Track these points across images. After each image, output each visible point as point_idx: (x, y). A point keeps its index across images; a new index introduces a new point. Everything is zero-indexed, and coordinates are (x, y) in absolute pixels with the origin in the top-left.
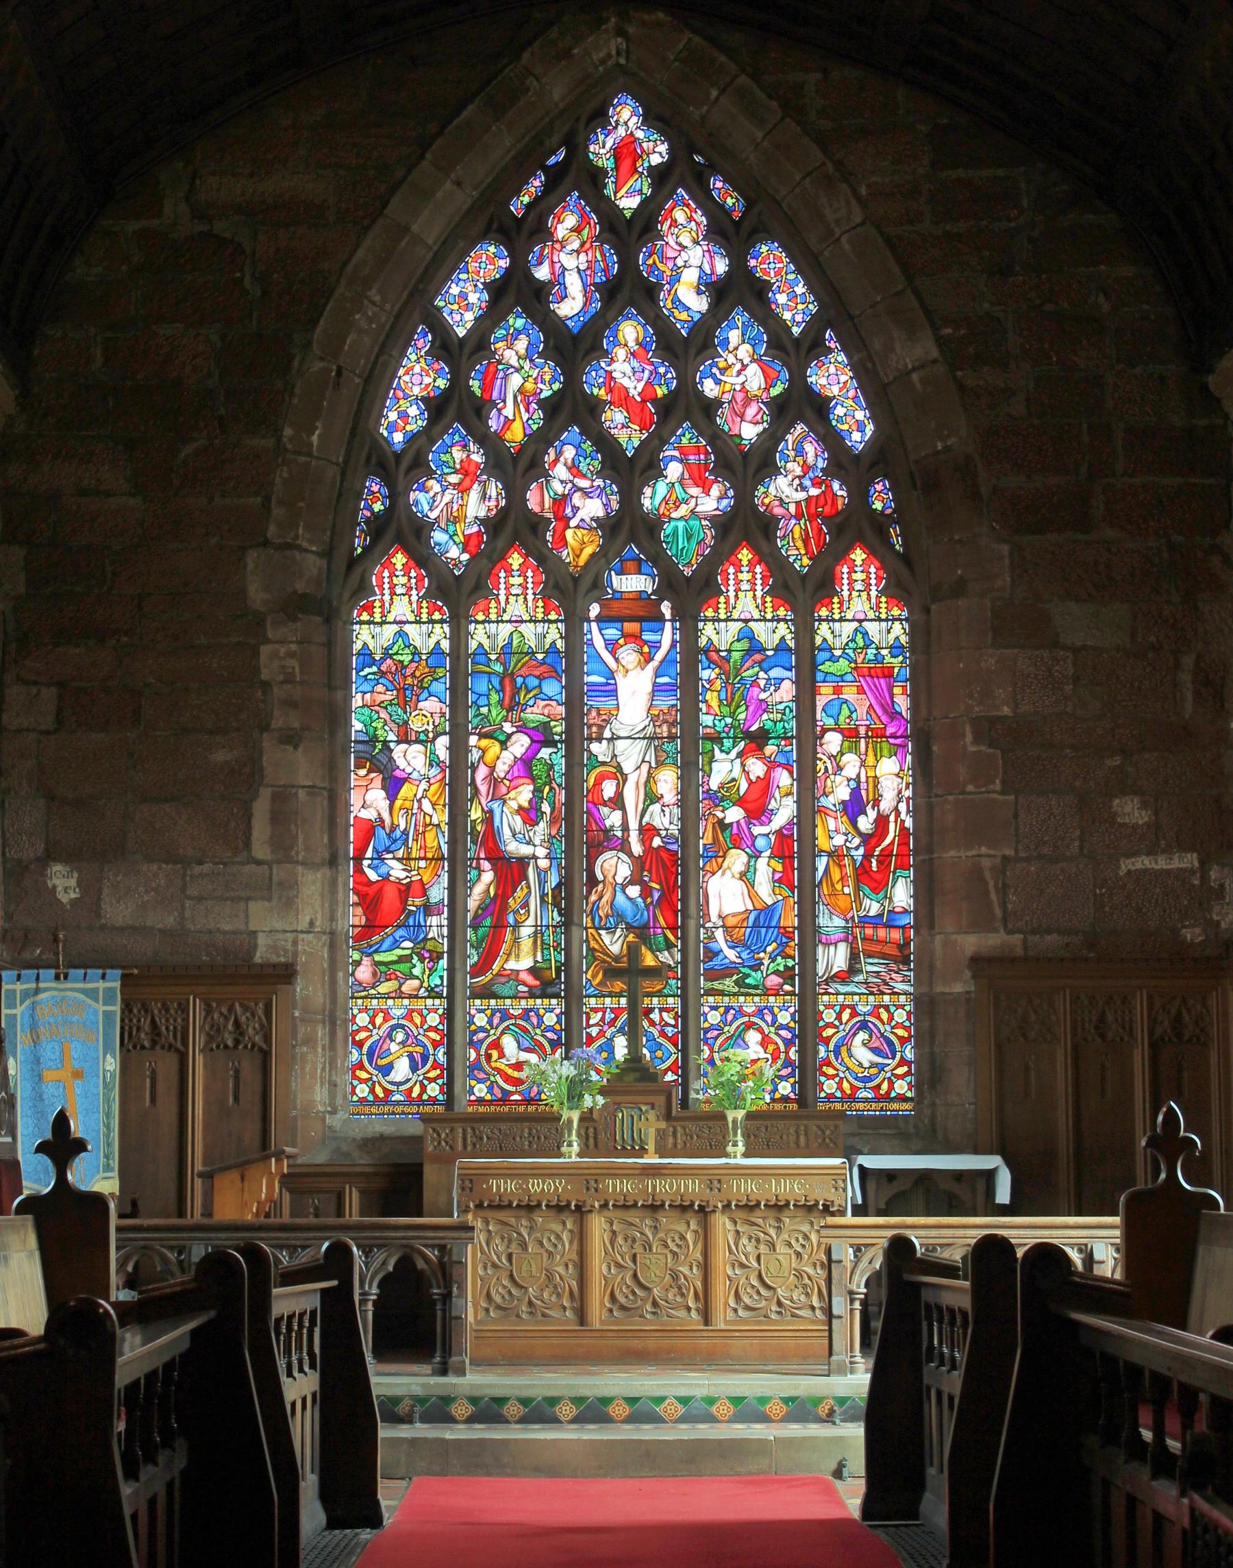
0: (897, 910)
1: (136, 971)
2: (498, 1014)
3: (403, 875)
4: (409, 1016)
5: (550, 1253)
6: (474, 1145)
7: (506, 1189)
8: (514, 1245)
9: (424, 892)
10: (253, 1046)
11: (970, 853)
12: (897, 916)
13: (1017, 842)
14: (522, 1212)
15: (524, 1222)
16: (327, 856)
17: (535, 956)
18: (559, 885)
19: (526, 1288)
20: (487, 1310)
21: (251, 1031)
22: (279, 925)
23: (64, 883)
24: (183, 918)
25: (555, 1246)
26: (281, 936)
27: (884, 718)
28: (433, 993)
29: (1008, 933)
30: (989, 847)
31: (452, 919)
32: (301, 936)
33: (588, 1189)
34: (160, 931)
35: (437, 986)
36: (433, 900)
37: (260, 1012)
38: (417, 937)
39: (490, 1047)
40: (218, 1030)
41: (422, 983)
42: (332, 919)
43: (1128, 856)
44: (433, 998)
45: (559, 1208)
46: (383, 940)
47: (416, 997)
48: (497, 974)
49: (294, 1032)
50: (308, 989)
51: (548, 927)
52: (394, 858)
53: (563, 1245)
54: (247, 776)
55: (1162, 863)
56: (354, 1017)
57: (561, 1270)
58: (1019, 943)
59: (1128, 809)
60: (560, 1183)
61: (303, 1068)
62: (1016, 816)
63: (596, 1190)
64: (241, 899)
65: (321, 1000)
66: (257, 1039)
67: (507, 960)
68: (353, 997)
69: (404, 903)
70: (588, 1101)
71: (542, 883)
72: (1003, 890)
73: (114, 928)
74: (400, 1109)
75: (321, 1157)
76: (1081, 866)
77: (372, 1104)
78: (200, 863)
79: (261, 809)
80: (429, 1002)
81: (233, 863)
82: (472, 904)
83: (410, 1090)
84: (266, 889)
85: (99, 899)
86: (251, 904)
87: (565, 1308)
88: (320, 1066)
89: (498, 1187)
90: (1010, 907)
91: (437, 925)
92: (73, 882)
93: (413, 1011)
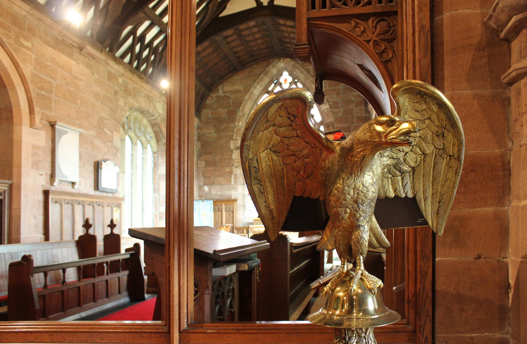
50: (239, 202)
54: (231, 172)
79: (233, 177)
84: (233, 188)
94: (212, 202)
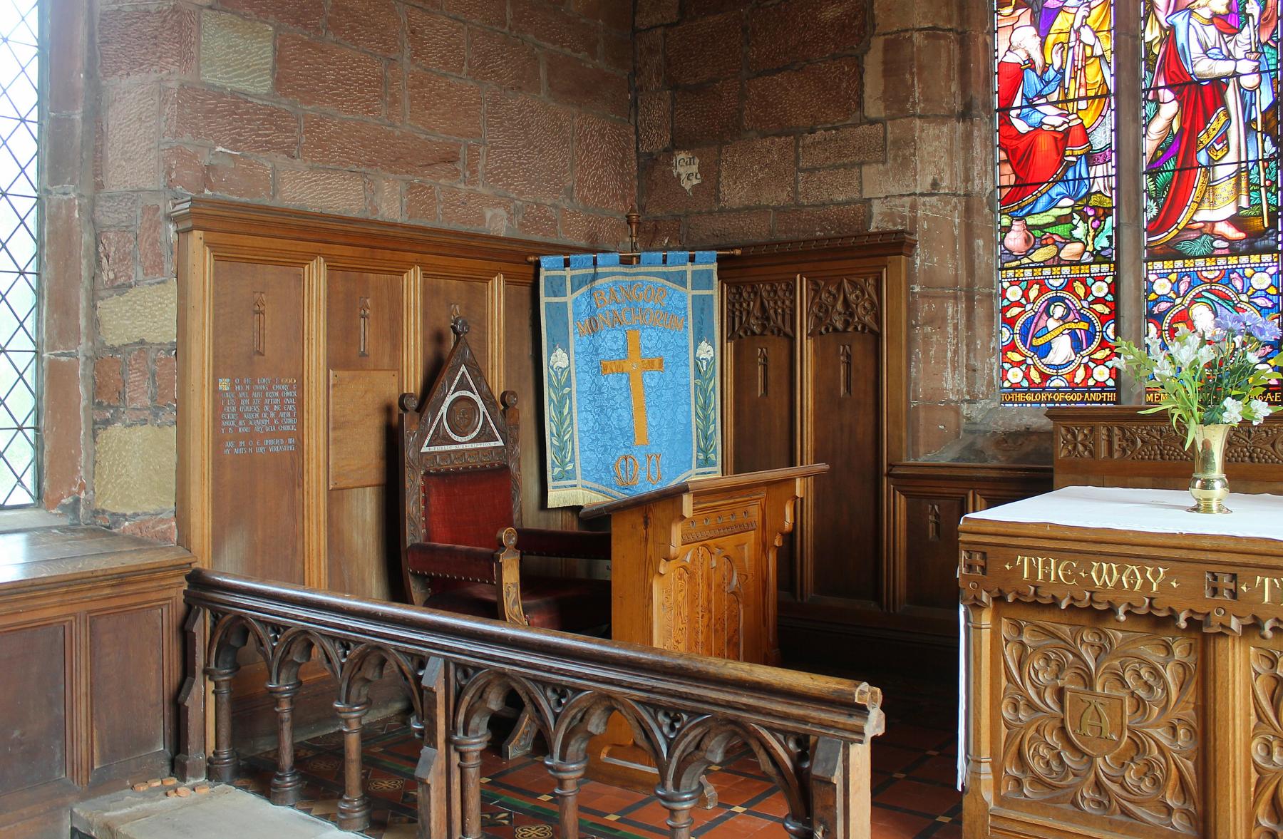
1: (738, 252)
2: (1186, 279)
3: (1057, 121)
4: (1069, 287)
5: (1139, 703)
6: (1124, 450)
7: (1047, 576)
8: (1068, 675)
9: (1086, 136)
10: (864, 328)
14: (1084, 620)
15: (1088, 637)
16: (958, 107)
17: (1237, 200)
18: (1273, 106)
19: (1091, 760)
20: (1018, 782)
21: (860, 311)
22: (895, 191)
23: (687, 170)
24: (796, 192)
25: (1150, 688)
26: (897, 201)
28: (1098, 257)
31: (1117, 167)
32: (923, 199)
33: (1215, 591)
34: (774, 208)
35: (1103, 249)
36: (1097, 146)
37: (870, 289)
38: (1078, 192)
39: (1176, 319)
40: (827, 310)
41: (1085, 246)
42: (967, 179)
44: (1100, 263)
45: (1157, 622)
46: (1037, 200)
47: (1078, 263)
48: (1184, 229)
49: (912, 310)
50: (932, 259)
51: (1256, 162)
52: (1048, 103)
53: (1166, 689)
56: (1004, 291)
57: (1161, 735)
60: (1155, 574)
61: (926, 352)
63: (1234, 594)
64: (853, 165)
65: (951, 272)
66: (867, 319)
67: (1197, 210)
68: (1002, 269)
69: (1062, 154)
70: (1233, 411)
71: (1246, 107)
73: (731, 210)
74: (1060, 397)
75: (946, 456)
77: (1028, 390)
78: (812, 131)
80: (1095, 268)
81: (845, 126)
82: (1149, 145)
83: (1074, 373)
85: (718, 182)
86: (865, 169)
87: (1169, 811)
88: (950, 349)
89: (1033, 571)
91: (1101, 176)
92: (694, 169)
93: (1075, 280)
94: (708, 263)
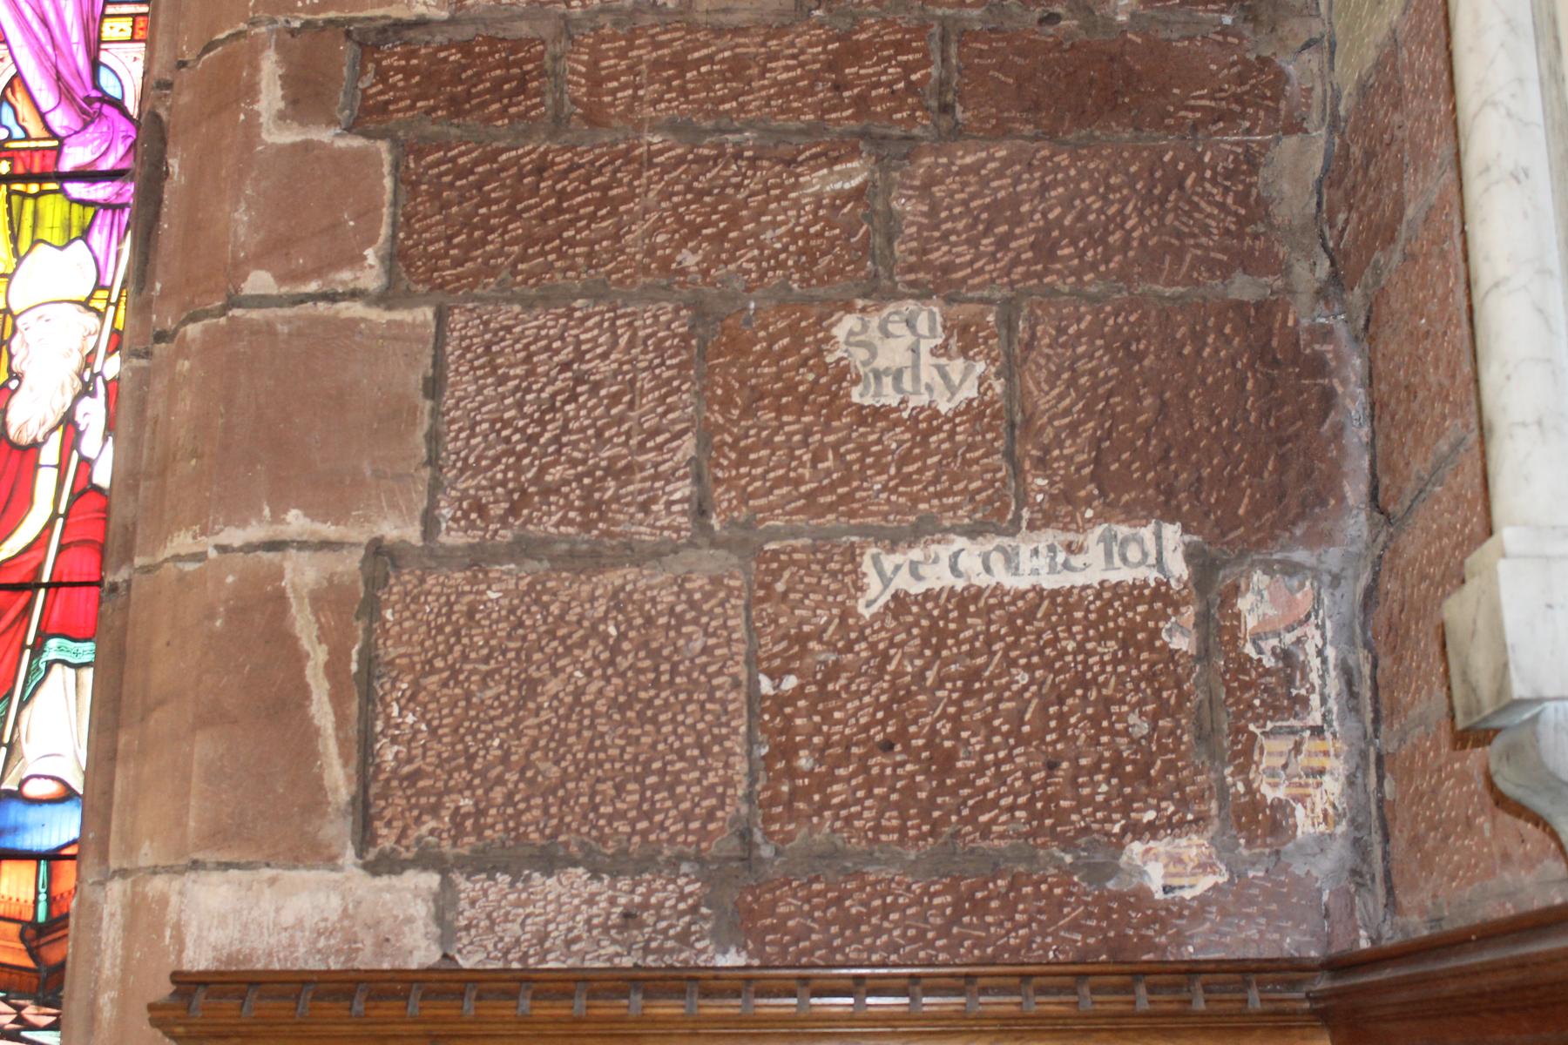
0: (32, 790)
11: (235, 536)
12: (33, 815)
13: (435, 487)
27: (60, 120)
29: (374, 868)
30: (310, 511)
43: (894, 540)
55: (1031, 565)
58: (421, 910)
59: (893, 354)
62: (434, 387)
72: (362, 687)
76: (698, 582)
90: (389, 754)
